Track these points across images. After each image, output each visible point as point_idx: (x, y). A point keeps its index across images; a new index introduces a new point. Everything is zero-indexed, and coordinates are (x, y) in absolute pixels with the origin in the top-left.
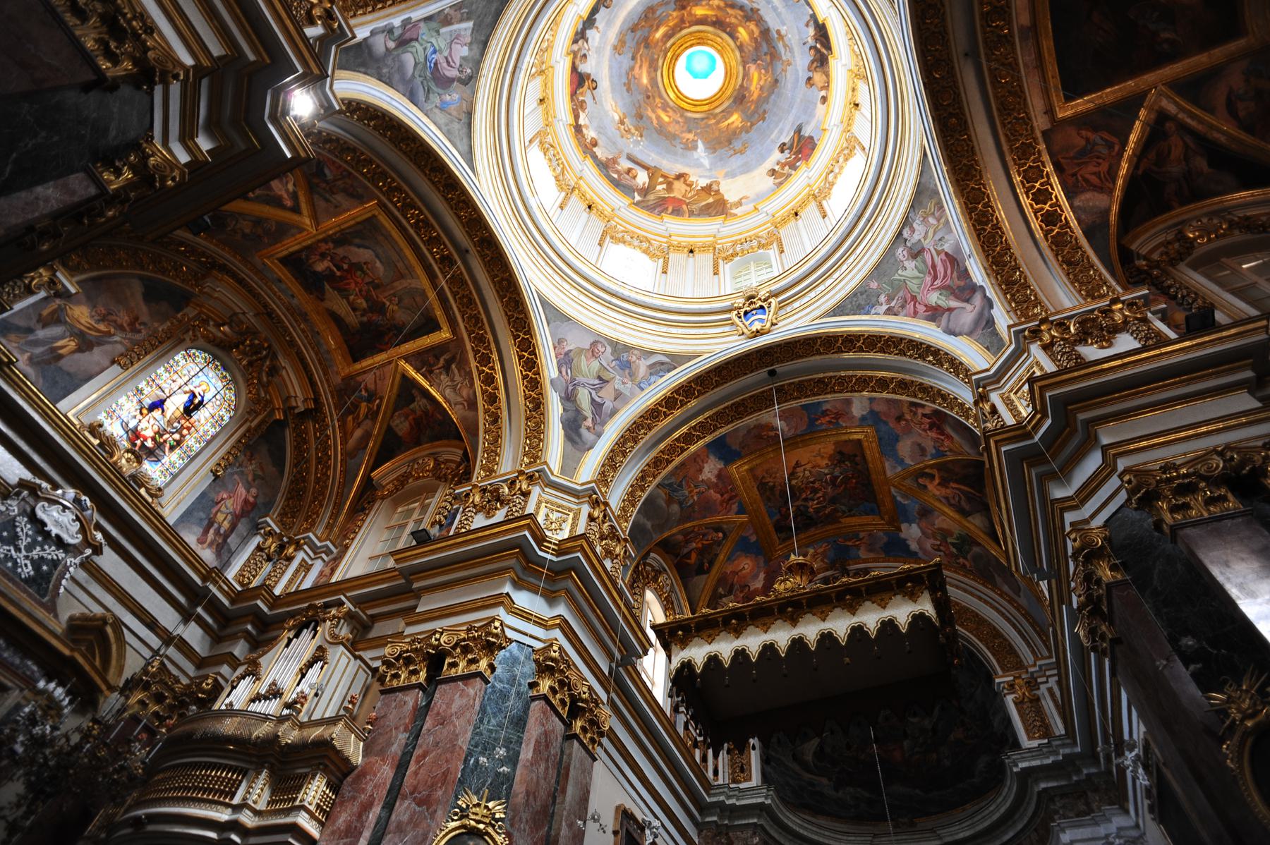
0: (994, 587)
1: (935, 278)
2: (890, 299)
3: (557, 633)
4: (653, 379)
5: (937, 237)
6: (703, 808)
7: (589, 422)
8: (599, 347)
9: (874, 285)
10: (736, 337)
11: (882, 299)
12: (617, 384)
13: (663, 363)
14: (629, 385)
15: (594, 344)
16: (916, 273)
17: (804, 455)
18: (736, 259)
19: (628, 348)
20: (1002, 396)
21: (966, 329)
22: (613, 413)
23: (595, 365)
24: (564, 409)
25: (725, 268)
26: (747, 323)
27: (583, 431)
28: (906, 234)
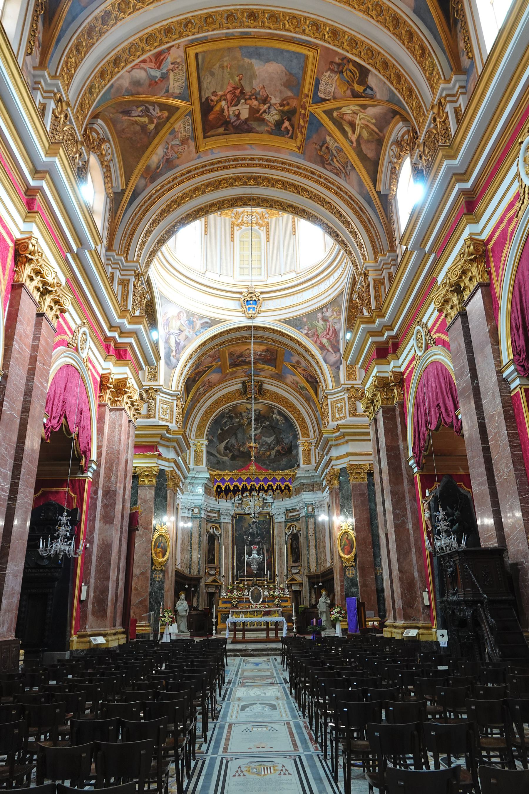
0: (309, 404)
1: (328, 334)
2: (308, 330)
3: (173, 465)
4: (202, 330)
5: (335, 321)
6: (185, 478)
7: (174, 353)
8: (181, 314)
9: (305, 320)
10: (240, 314)
11: (306, 327)
12: (187, 333)
13: (207, 323)
14: (191, 333)
15: (179, 313)
16: (322, 327)
17: (252, 347)
18: (243, 227)
19: (193, 315)
20: (331, 402)
21: (331, 363)
22: (184, 347)
23: (178, 323)
24: (165, 348)
25: (238, 234)
26: (247, 307)
27: (172, 358)
28: (324, 310)
